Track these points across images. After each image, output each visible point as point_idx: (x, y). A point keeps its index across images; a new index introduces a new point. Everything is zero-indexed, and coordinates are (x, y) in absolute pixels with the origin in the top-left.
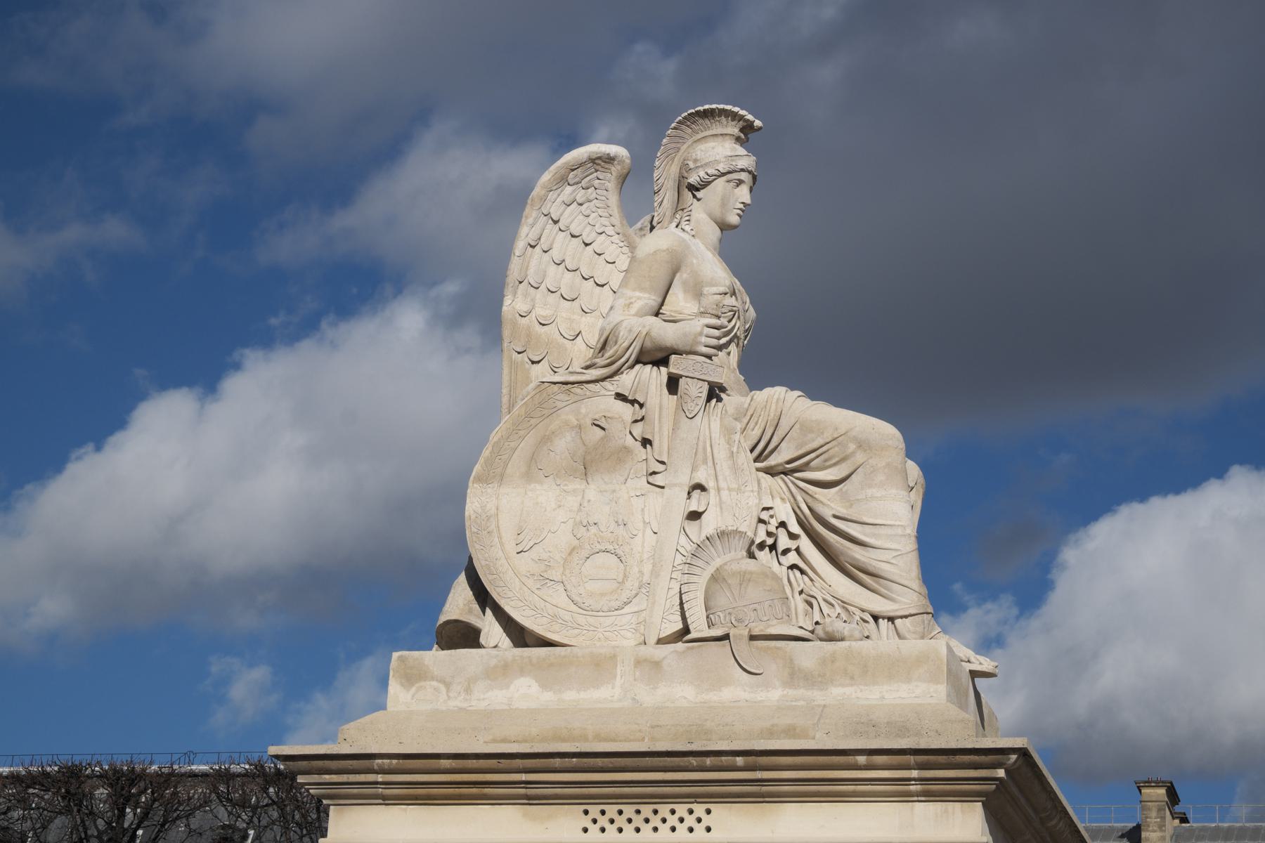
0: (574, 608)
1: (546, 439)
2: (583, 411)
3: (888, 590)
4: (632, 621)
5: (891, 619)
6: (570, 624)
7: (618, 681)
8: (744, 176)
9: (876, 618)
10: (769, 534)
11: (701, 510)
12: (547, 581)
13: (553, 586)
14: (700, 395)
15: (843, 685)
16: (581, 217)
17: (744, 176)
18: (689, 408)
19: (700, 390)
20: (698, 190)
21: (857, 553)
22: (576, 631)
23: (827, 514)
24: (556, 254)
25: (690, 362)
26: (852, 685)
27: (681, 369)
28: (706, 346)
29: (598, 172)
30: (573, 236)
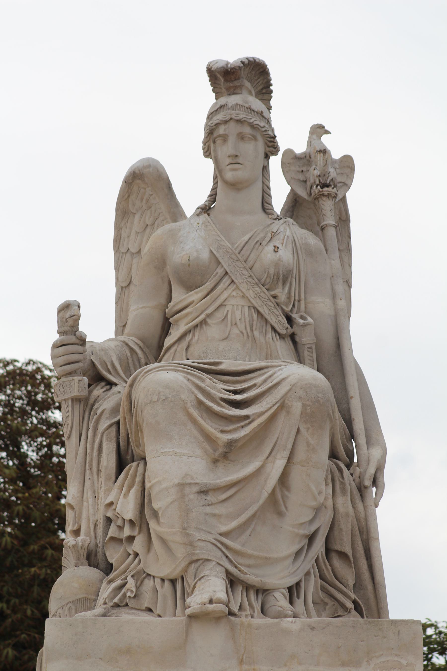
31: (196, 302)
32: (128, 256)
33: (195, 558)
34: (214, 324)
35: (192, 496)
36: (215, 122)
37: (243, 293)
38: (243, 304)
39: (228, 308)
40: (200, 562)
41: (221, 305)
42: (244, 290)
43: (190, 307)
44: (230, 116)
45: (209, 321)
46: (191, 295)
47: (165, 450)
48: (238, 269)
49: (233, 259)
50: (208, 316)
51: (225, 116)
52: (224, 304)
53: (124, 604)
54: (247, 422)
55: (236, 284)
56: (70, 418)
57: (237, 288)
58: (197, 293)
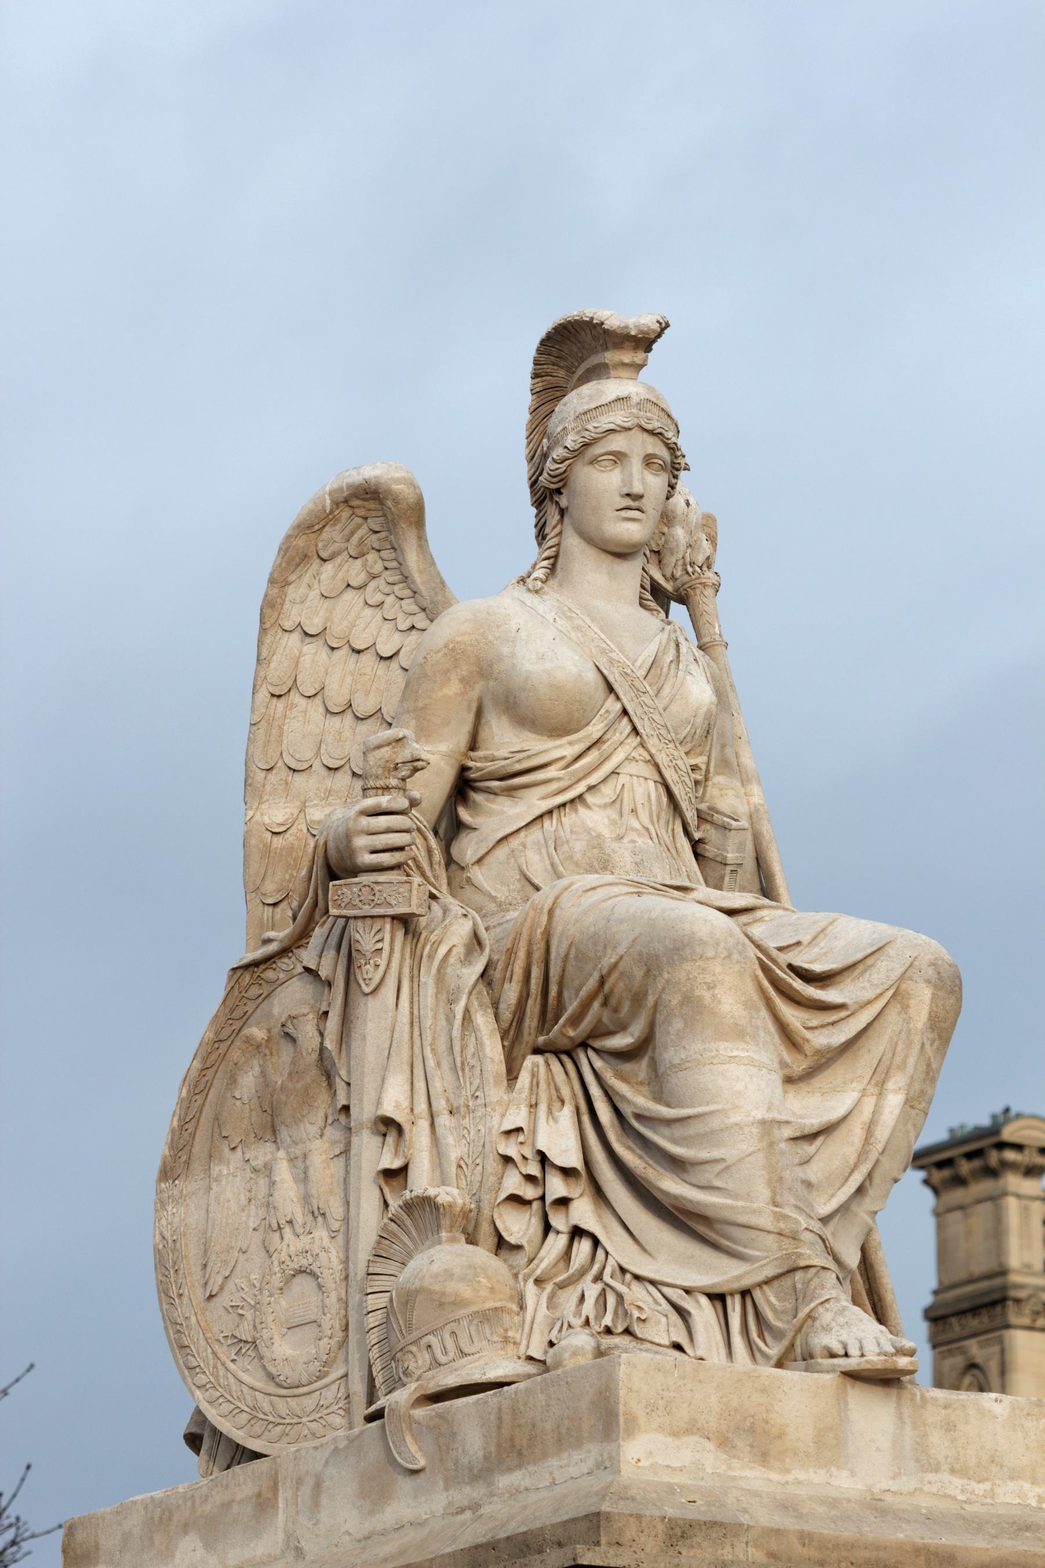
0: (272, 1388)
1: (233, 1081)
2: (276, 1011)
3: (728, 1238)
4: (339, 1396)
5: (745, 1293)
6: (271, 1418)
7: (281, 1517)
8: (617, 443)
9: (718, 1298)
10: (530, 1178)
11: (396, 1164)
12: (242, 1344)
13: (249, 1353)
14: (379, 946)
15: (510, 1470)
16: (368, 612)
17: (617, 443)
18: (366, 977)
19: (377, 938)
20: (559, 491)
21: (670, 1185)
22: (279, 1428)
23: (627, 1111)
24: (337, 698)
25: (355, 890)
26: (519, 1467)
27: (343, 905)
28: (373, 852)
29: (369, 520)
30: (359, 652)
31: (569, 759)
32: (296, 637)
33: (802, 1263)
34: (599, 807)
35: (783, 1145)
36: (605, 426)
37: (651, 755)
38: (647, 776)
39: (622, 779)
40: (813, 1271)
41: (614, 773)
42: (653, 751)
43: (552, 768)
44: (636, 419)
45: (589, 798)
46: (560, 746)
47: (735, 1053)
48: (646, 709)
49: (638, 690)
50: (591, 788)
51: (626, 420)
52: (617, 771)
53: (620, 1329)
54: (843, 1014)
55: (641, 737)
56: (385, 954)
57: (642, 745)
58: (570, 743)
